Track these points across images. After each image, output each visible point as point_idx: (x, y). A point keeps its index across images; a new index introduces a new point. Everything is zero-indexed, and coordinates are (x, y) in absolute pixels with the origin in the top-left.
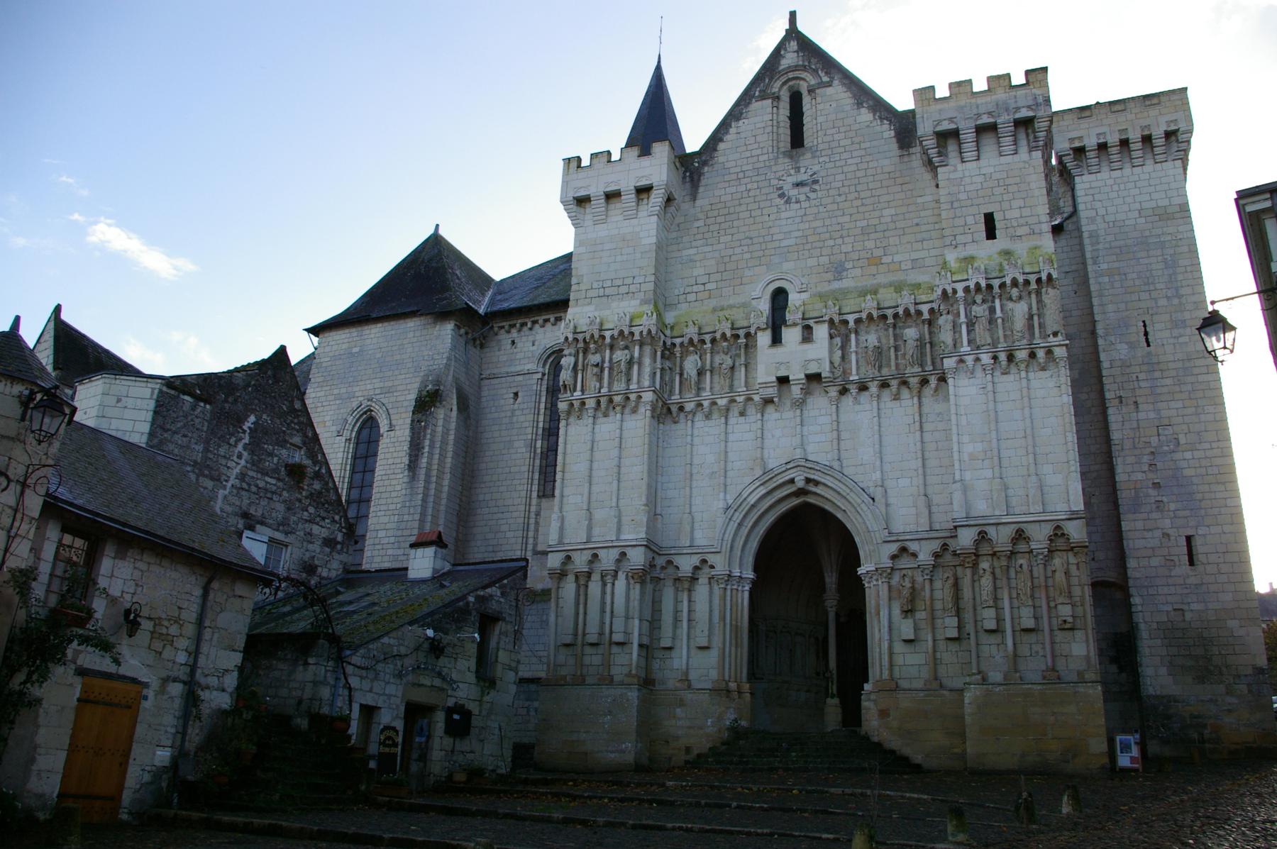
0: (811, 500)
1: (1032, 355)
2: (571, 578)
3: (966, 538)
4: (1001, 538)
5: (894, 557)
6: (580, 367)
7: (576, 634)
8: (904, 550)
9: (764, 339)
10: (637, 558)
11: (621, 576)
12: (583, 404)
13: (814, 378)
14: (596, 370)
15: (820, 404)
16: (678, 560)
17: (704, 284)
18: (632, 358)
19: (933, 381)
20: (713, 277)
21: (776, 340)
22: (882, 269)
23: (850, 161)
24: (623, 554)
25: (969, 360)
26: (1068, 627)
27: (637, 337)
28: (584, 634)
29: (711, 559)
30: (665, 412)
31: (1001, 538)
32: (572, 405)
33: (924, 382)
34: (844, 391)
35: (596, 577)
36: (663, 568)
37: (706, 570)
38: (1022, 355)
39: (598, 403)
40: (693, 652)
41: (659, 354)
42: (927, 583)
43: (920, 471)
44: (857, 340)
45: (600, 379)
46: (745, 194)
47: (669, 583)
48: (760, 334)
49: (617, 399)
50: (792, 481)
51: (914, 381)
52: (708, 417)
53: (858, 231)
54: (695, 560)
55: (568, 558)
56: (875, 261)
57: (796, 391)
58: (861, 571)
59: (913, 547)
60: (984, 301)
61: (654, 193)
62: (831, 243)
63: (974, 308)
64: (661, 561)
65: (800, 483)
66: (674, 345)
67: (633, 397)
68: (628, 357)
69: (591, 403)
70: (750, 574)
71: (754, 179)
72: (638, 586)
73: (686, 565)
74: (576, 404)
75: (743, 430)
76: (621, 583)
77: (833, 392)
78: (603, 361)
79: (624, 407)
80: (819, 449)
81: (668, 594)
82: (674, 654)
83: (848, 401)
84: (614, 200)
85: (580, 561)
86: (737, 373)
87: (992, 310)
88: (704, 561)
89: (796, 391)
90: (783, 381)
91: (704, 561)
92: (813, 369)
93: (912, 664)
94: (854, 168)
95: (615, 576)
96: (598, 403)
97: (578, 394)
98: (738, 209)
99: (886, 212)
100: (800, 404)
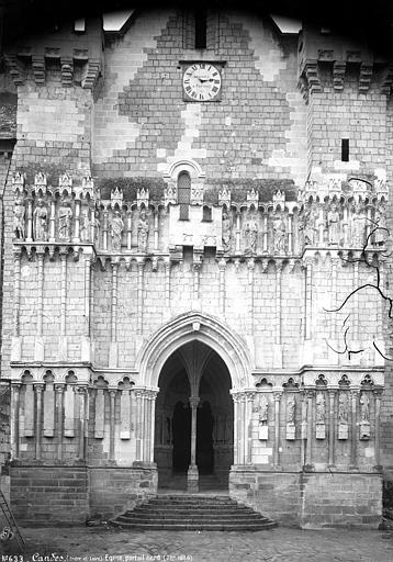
0: (200, 339)
1: (364, 254)
2: (29, 388)
3: (310, 380)
4: (333, 381)
5: (258, 385)
6: (30, 217)
7: (35, 430)
8: (264, 381)
9: (175, 212)
10: (83, 376)
11: (70, 388)
12: (34, 249)
13: (210, 251)
14: (43, 221)
15: (212, 268)
16: (106, 377)
17: (125, 157)
18: (74, 214)
19: (292, 262)
20: (133, 153)
21: (184, 218)
22: (261, 168)
23: (243, 70)
24: (71, 373)
25: (323, 253)
26: (365, 440)
27: (77, 197)
28: (42, 429)
29: (132, 378)
30: (100, 265)
31: (333, 381)
32: (24, 249)
33: (286, 262)
34: (230, 260)
35: (50, 388)
36: (95, 381)
37: (128, 386)
38: (358, 255)
39: (47, 249)
40: (118, 443)
41: (93, 214)
42: (277, 403)
43: (278, 327)
44: (241, 223)
45: (47, 230)
46: (159, 82)
47: (100, 392)
48: (171, 208)
49: (63, 250)
50: (191, 325)
51: (279, 262)
52: (128, 270)
53: (244, 134)
54: (120, 378)
55: (27, 372)
56: (256, 161)
57: (197, 259)
58: (231, 391)
59: (270, 379)
60: (337, 210)
61: (87, 67)
62: (225, 140)
63: (330, 214)
64: (95, 377)
65: (196, 327)
66: (102, 207)
67: (76, 249)
68: (71, 213)
69: (40, 250)
70: (158, 389)
71: (167, 69)
72: (82, 397)
73: (113, 382)
74: (29, 248)
75: (158, 282)
76: (70, 393)
77: (223, 262)
78: (49, 214)
79: (67, 256)
80: (209, 306)
81: (101, 398)
82: (103, 443)
83: (233, 268)
84: (54, 67)
85: (38, 376)
86: (151, 239)
87: (341, 217)
88: (126, 379)
89: (197, 259)
90: (188, 250)
91: (126, 379)
92: (210, 244)
93: (263, 456)
94: (246, 77)
95: (65, 389)
96: (47, 249)
97: (29, 240)
98: (153, 94)
99: (267, 122)
100: (199, 268)
